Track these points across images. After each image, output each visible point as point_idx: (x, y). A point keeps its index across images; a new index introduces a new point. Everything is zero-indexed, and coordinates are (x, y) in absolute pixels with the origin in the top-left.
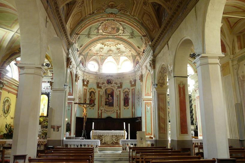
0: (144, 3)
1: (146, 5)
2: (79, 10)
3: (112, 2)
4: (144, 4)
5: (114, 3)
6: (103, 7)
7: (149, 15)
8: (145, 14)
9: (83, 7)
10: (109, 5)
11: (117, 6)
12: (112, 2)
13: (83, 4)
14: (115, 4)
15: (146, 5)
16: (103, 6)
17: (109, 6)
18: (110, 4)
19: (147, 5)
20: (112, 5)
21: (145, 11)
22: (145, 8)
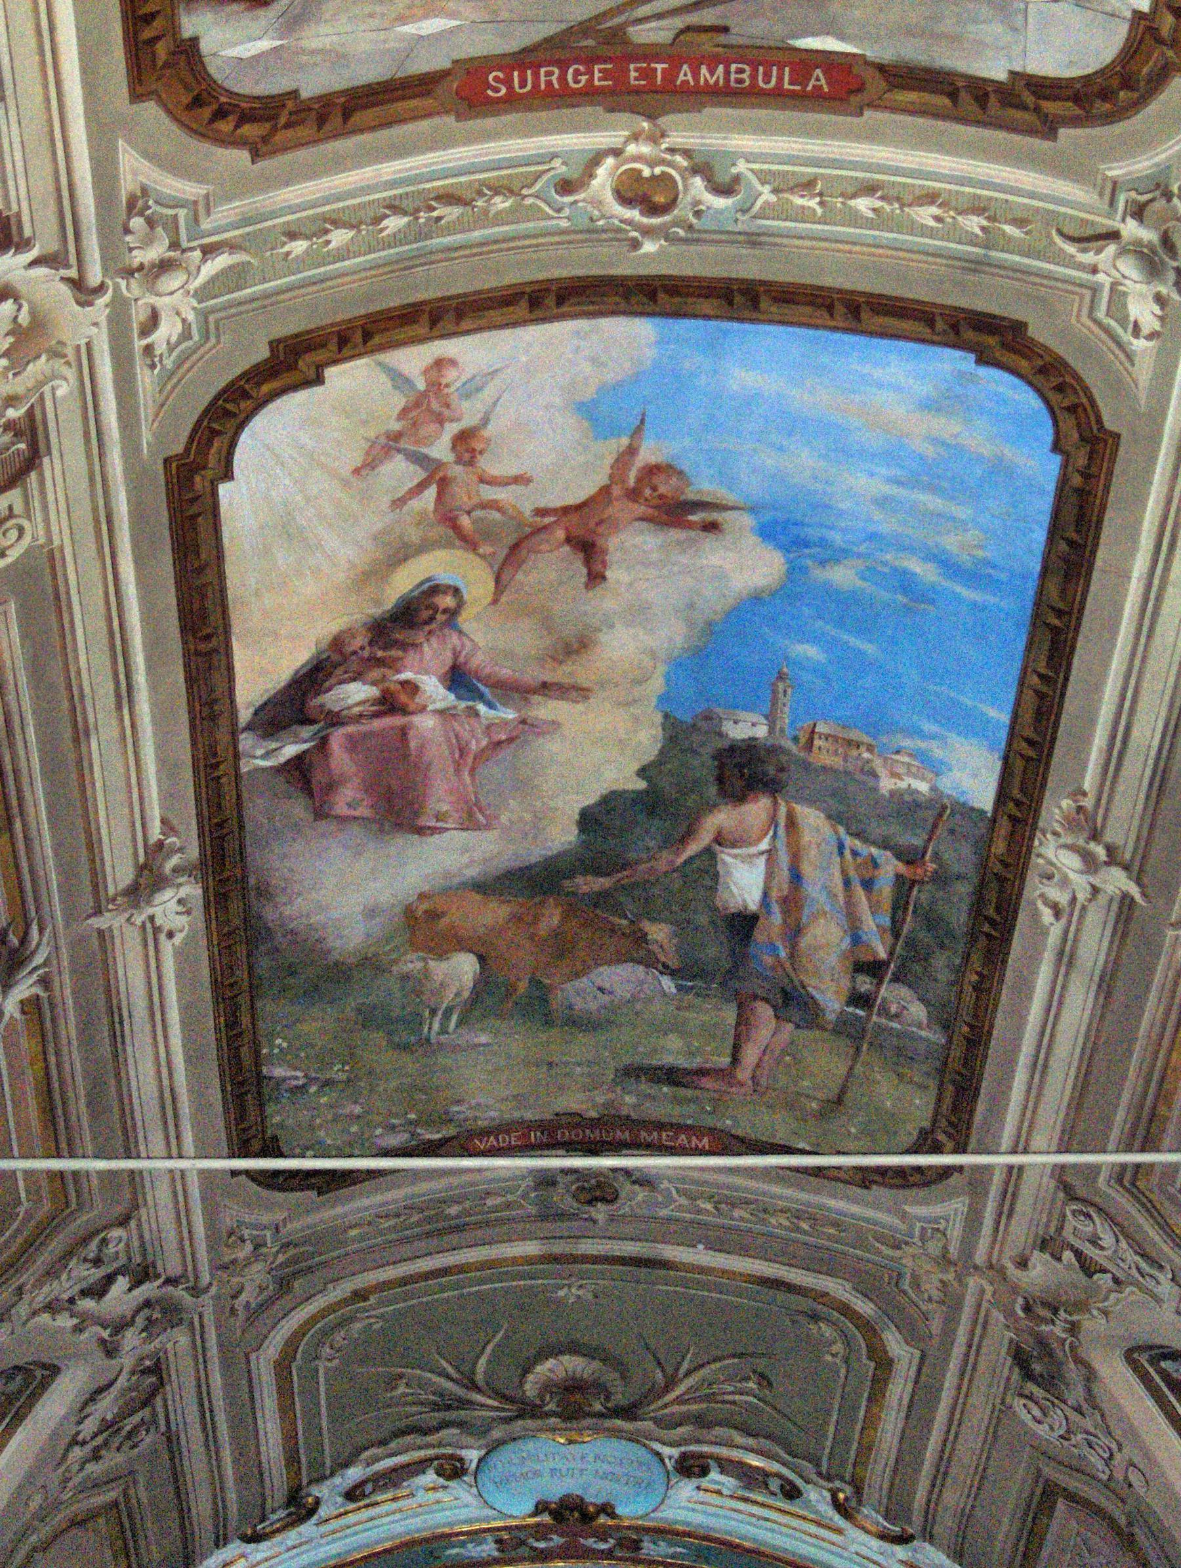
0: (1020, 1358)
1: (1051, 1382)
2: (96, 1485)
3: (575, 1348)
4: (1028, 1375)
5: (596, 1364)
6: (445, 1425)
7: (1111, 1521)
8: (1061, 1505)
9: (148, 1440)
10: (530, 1388)
11: (635, 1405)
12: (565, 1359)
13: (147, 1402)
14: (611, 1377)
15: (1051, 1382)
16: (436, 1407)
17: (529, 1410)
18: (548, 1387)
19: (1076, 1394)
20: (573, 1387)
21: (1048, 1471)
22: (1042, 1430)
